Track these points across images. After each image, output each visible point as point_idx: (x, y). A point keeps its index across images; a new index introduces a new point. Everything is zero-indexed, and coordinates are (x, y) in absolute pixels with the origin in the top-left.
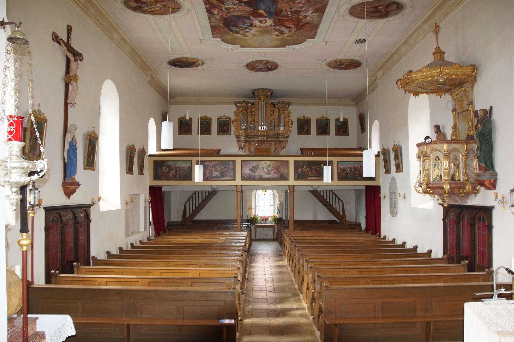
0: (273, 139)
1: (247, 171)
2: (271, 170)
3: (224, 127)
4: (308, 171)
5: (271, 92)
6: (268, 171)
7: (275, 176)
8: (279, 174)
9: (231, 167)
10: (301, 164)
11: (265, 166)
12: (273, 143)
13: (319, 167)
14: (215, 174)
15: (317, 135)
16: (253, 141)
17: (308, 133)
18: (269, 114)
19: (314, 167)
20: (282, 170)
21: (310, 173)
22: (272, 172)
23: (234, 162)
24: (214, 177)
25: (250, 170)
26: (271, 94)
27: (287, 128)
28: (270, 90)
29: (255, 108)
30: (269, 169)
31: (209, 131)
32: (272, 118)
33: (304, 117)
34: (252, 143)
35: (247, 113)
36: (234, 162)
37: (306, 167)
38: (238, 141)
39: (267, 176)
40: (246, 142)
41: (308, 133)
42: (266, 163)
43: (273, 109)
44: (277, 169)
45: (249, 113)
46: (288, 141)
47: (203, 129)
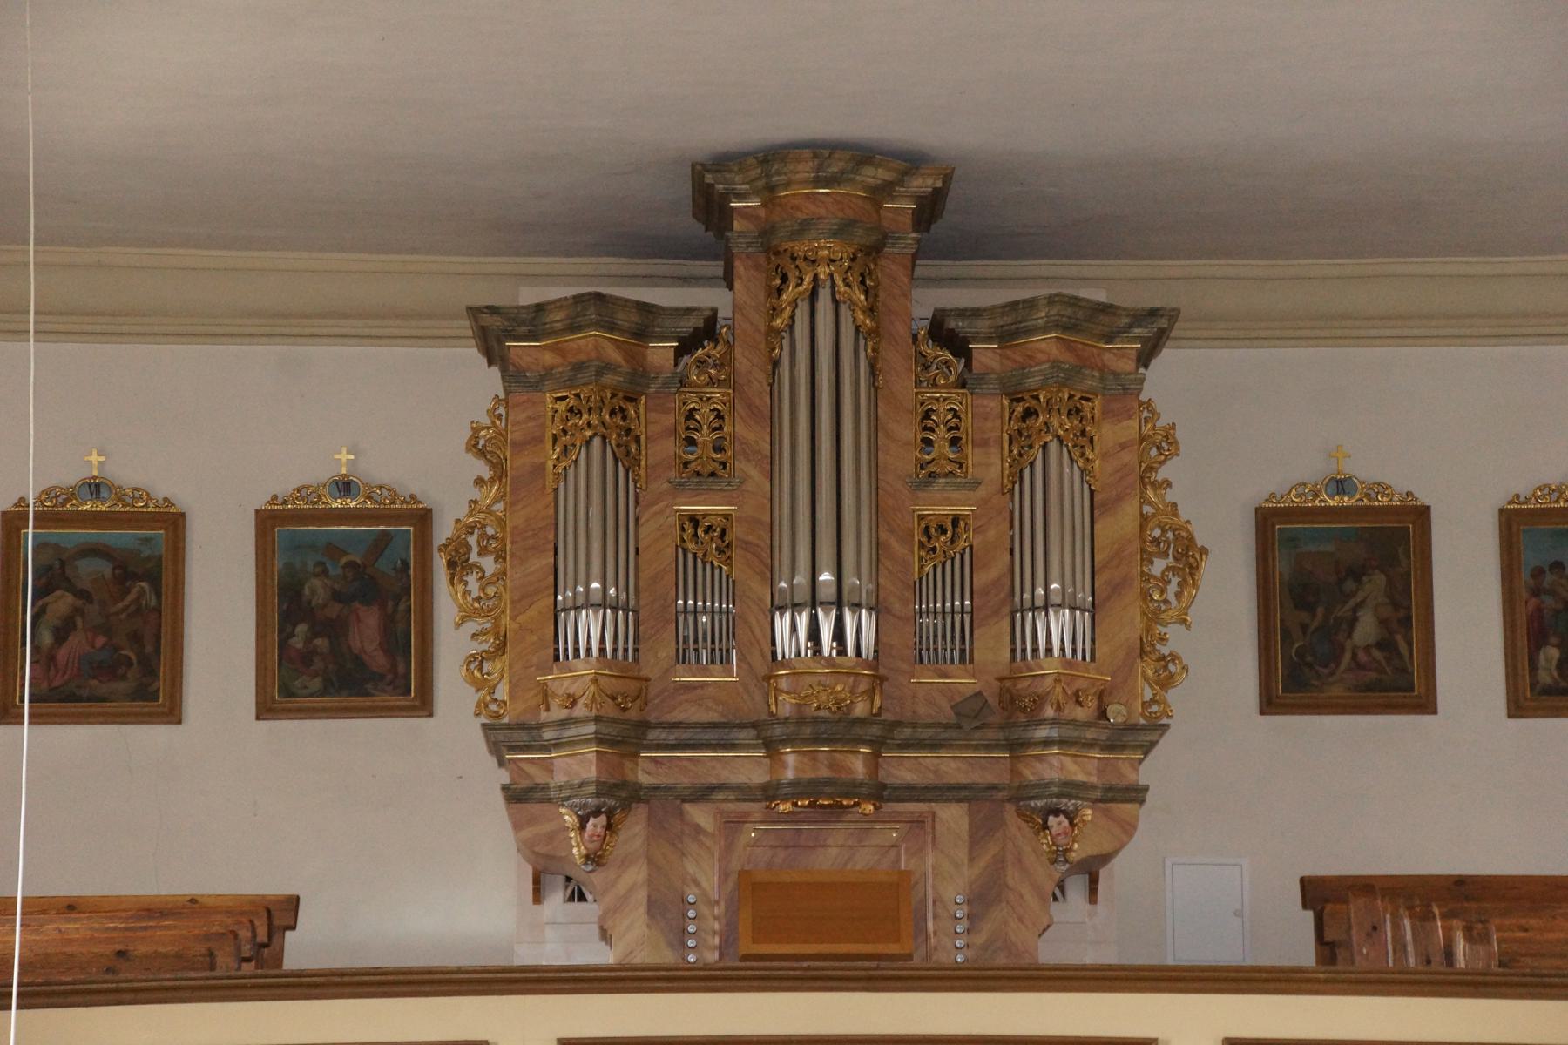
0: (951, 766)
3: (346, 621)
5: (924, 183)
12: (953, 817)
15: (1517, 709)
16: (703, 794)
17: (1396, 679)
18: (901, 459)
26: (930, 209)
27: (1127, 621)
28: (911, 161)
29: (730, 382)
31: (149, 669)
32: (940, 504)
33: (1341, 485)
34: (701, 815)
35: (627, 452)
38: (516, 796)
40: (615, 800)
41: (1396, 679)
43: (945, 400)
45: (661, 450)
46: (1136, 794)
47: (77, 642)
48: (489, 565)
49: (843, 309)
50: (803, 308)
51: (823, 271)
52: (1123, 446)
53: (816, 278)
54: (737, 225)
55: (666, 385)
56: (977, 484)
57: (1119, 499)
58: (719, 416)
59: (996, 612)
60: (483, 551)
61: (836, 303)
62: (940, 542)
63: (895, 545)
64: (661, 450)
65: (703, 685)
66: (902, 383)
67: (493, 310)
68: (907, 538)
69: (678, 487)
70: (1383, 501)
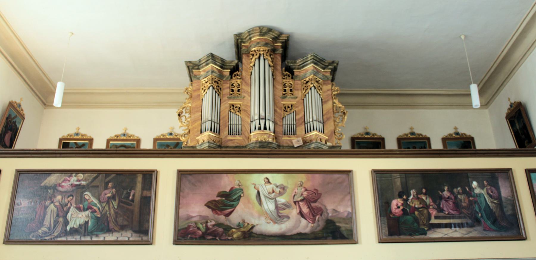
1: (197, 210)
2: (287, 206)
4: (426, 207)
5: (283, 38)
6: (277, 207)
7: (305, 226)
8: (320, 222)
9: (137, 192)
10: (398, 182)
11: (265, 189)
13: (464, 192)
14: (77, 218)
18: (280, 93)
19: (446, 194)
20: (332, 206)
21: (434, 213)
22: (294, 212)
23: (149, 177)
24: (74, 231)
25: (213, 206)
28: (281, 34)
30: (282, 200)
32: (287, 102)
33: (367, 133)
35: (218, 90)
36: (149, 177)
37: (419, 192)
39: (274, 228)
42: (268, 181)
43: (289, 81)
44: (311, 201)
45: (226, 92)
48: (187, 115)
49: (266, 61)
50: (257, 61)
51: (262, 53)
52: (328, 90)
53: (260, 54)
54: (243, 48)
55: (227, 78)
56: (297, 98)
57: (328, 101)
58: (239, 85)
59: (301, 124)
60: (186, 113)
61: (264, 59)
62: (288, 110)
63: (278, 110)
64: (226, 92)
65: (234, 139)
66: (279, 78)
67: (190, 62)
68: (281, 109)
69: (230, 98)
70: (376, 136)
